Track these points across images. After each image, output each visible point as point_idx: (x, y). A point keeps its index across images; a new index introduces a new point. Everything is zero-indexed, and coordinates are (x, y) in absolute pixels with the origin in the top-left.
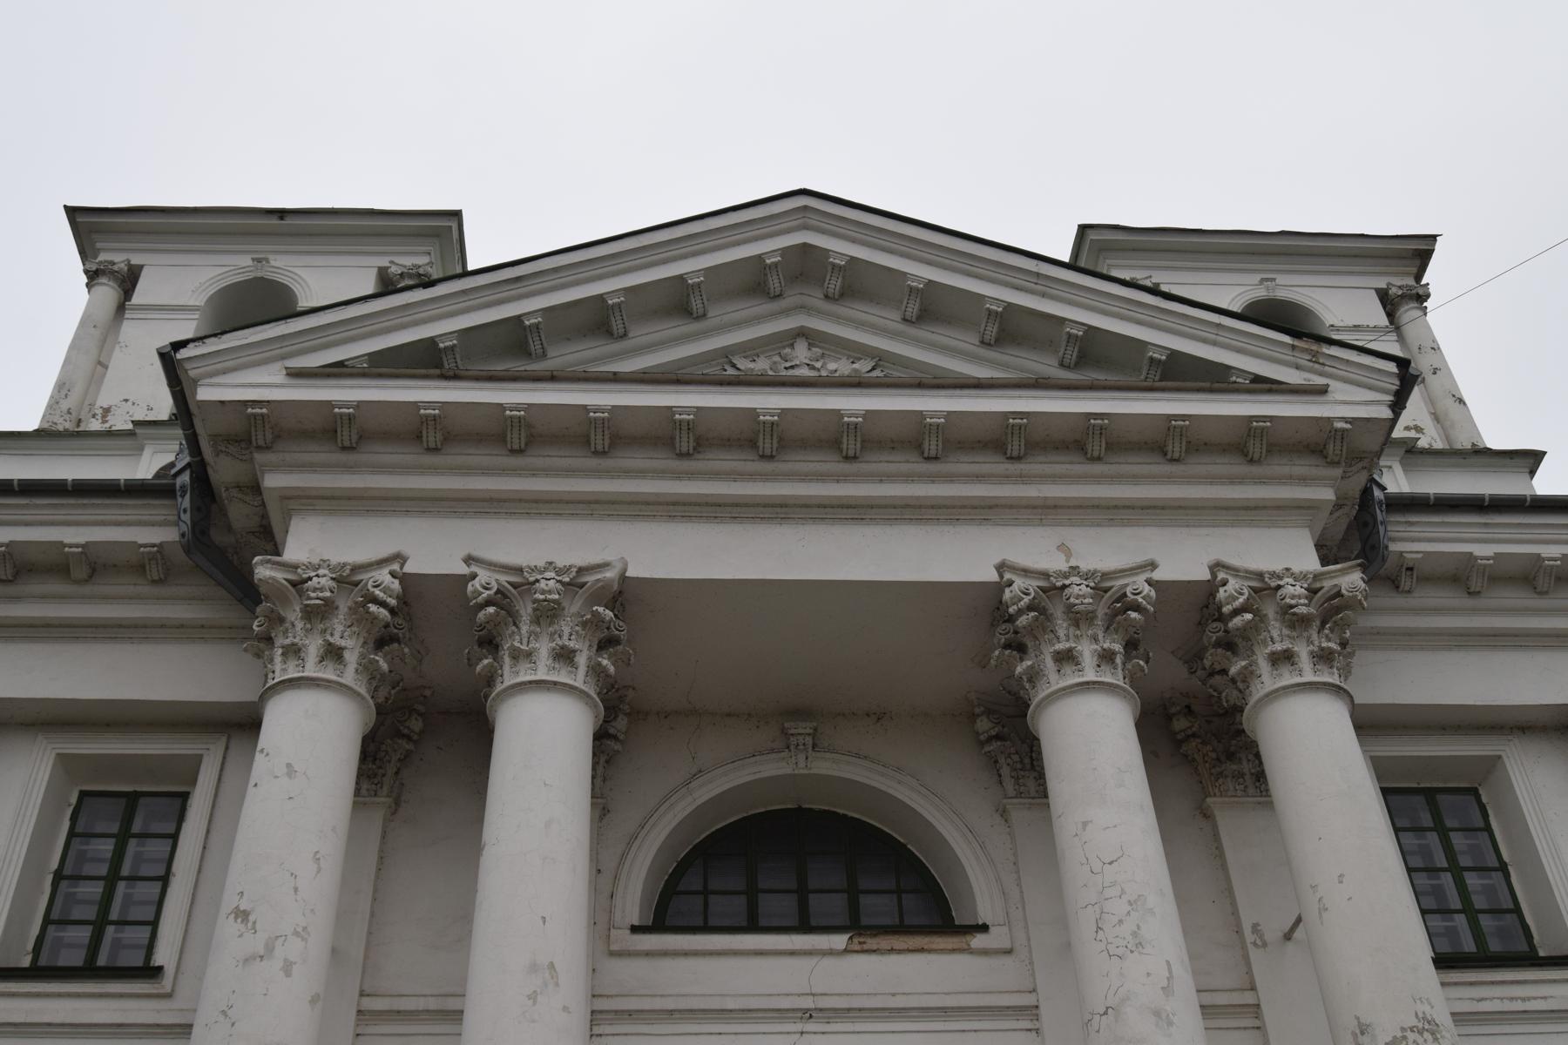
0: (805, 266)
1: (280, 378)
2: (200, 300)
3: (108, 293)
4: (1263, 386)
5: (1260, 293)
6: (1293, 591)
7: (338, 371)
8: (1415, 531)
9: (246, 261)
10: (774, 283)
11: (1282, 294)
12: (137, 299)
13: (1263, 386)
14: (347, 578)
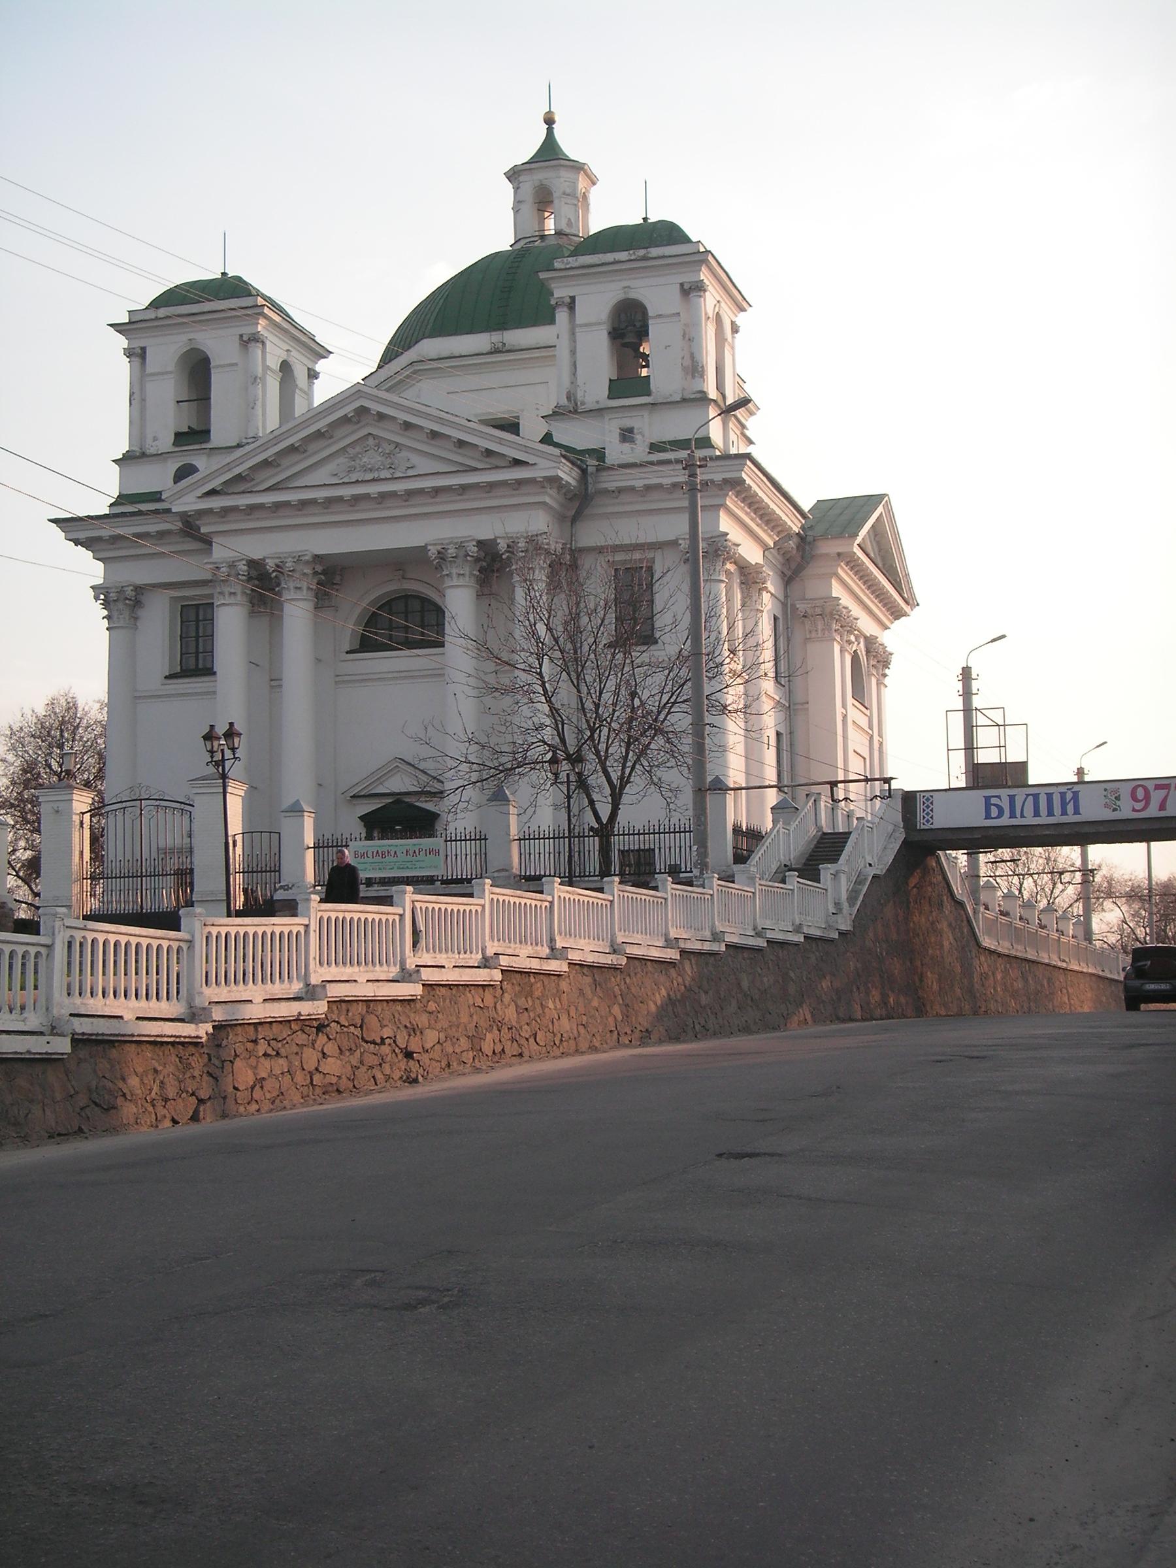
0: (362, 411)
1: (194, 500)
2: (171, 367)
3: (137, 360)
4: (517, 463)
5: (621, 296)
6: (522, 544)
7: (213, 493)
8: (612, 478)
9: (184, 338)
10: (354, 420)
11: (633, 295)
12: (150, 369)
13: (517, 463)
14: (232, 565)
